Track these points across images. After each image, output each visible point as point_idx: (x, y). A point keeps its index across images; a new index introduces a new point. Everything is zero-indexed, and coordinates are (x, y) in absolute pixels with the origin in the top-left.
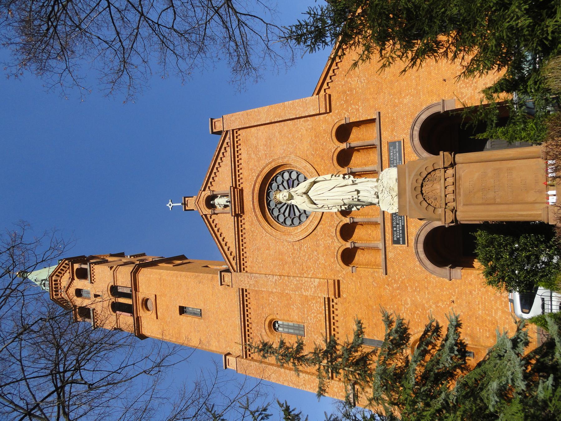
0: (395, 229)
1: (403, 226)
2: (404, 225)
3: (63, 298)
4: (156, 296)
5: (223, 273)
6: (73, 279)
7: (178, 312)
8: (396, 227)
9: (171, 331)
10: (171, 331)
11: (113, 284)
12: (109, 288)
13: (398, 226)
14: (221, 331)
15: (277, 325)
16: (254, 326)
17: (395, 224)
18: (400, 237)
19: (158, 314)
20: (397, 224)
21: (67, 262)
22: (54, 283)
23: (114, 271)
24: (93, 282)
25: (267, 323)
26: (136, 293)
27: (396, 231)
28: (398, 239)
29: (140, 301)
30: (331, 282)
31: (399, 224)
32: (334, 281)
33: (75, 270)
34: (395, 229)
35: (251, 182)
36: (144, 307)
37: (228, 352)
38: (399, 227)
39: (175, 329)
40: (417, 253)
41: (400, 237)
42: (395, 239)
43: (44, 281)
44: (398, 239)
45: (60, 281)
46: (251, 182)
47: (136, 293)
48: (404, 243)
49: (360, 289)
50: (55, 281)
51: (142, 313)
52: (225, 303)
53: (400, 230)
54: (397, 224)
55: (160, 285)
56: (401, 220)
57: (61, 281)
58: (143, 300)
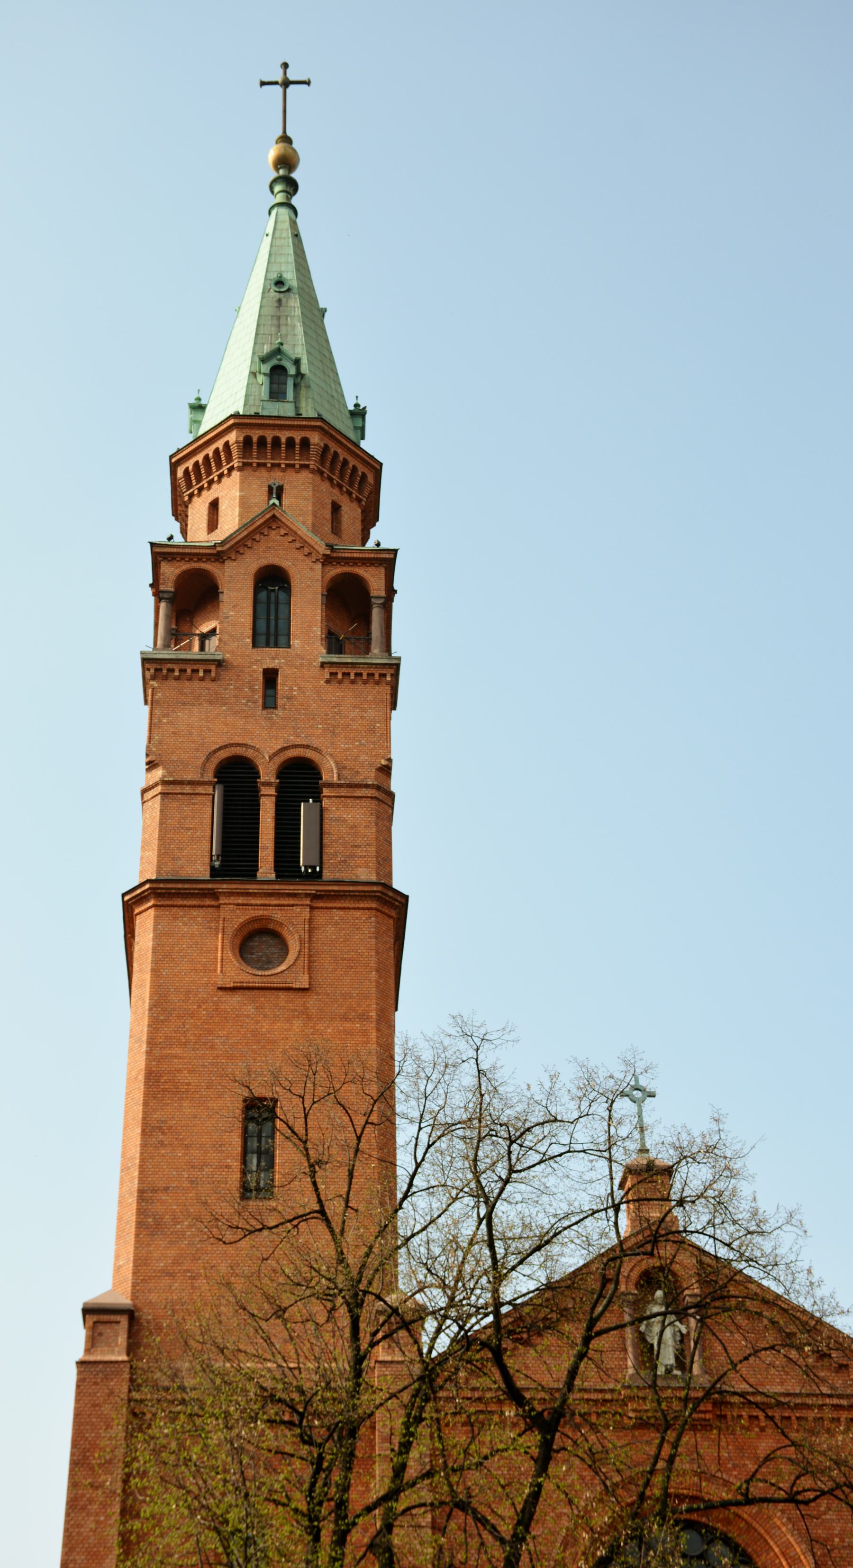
9: (178, 1051)
10: (178, 1051)
26: (307, 895)
29: (278, 915)
33: (361, 571)
35: (735, 1467)
46: (735, 1467)
50: (305, 443)
58: (281, 924)
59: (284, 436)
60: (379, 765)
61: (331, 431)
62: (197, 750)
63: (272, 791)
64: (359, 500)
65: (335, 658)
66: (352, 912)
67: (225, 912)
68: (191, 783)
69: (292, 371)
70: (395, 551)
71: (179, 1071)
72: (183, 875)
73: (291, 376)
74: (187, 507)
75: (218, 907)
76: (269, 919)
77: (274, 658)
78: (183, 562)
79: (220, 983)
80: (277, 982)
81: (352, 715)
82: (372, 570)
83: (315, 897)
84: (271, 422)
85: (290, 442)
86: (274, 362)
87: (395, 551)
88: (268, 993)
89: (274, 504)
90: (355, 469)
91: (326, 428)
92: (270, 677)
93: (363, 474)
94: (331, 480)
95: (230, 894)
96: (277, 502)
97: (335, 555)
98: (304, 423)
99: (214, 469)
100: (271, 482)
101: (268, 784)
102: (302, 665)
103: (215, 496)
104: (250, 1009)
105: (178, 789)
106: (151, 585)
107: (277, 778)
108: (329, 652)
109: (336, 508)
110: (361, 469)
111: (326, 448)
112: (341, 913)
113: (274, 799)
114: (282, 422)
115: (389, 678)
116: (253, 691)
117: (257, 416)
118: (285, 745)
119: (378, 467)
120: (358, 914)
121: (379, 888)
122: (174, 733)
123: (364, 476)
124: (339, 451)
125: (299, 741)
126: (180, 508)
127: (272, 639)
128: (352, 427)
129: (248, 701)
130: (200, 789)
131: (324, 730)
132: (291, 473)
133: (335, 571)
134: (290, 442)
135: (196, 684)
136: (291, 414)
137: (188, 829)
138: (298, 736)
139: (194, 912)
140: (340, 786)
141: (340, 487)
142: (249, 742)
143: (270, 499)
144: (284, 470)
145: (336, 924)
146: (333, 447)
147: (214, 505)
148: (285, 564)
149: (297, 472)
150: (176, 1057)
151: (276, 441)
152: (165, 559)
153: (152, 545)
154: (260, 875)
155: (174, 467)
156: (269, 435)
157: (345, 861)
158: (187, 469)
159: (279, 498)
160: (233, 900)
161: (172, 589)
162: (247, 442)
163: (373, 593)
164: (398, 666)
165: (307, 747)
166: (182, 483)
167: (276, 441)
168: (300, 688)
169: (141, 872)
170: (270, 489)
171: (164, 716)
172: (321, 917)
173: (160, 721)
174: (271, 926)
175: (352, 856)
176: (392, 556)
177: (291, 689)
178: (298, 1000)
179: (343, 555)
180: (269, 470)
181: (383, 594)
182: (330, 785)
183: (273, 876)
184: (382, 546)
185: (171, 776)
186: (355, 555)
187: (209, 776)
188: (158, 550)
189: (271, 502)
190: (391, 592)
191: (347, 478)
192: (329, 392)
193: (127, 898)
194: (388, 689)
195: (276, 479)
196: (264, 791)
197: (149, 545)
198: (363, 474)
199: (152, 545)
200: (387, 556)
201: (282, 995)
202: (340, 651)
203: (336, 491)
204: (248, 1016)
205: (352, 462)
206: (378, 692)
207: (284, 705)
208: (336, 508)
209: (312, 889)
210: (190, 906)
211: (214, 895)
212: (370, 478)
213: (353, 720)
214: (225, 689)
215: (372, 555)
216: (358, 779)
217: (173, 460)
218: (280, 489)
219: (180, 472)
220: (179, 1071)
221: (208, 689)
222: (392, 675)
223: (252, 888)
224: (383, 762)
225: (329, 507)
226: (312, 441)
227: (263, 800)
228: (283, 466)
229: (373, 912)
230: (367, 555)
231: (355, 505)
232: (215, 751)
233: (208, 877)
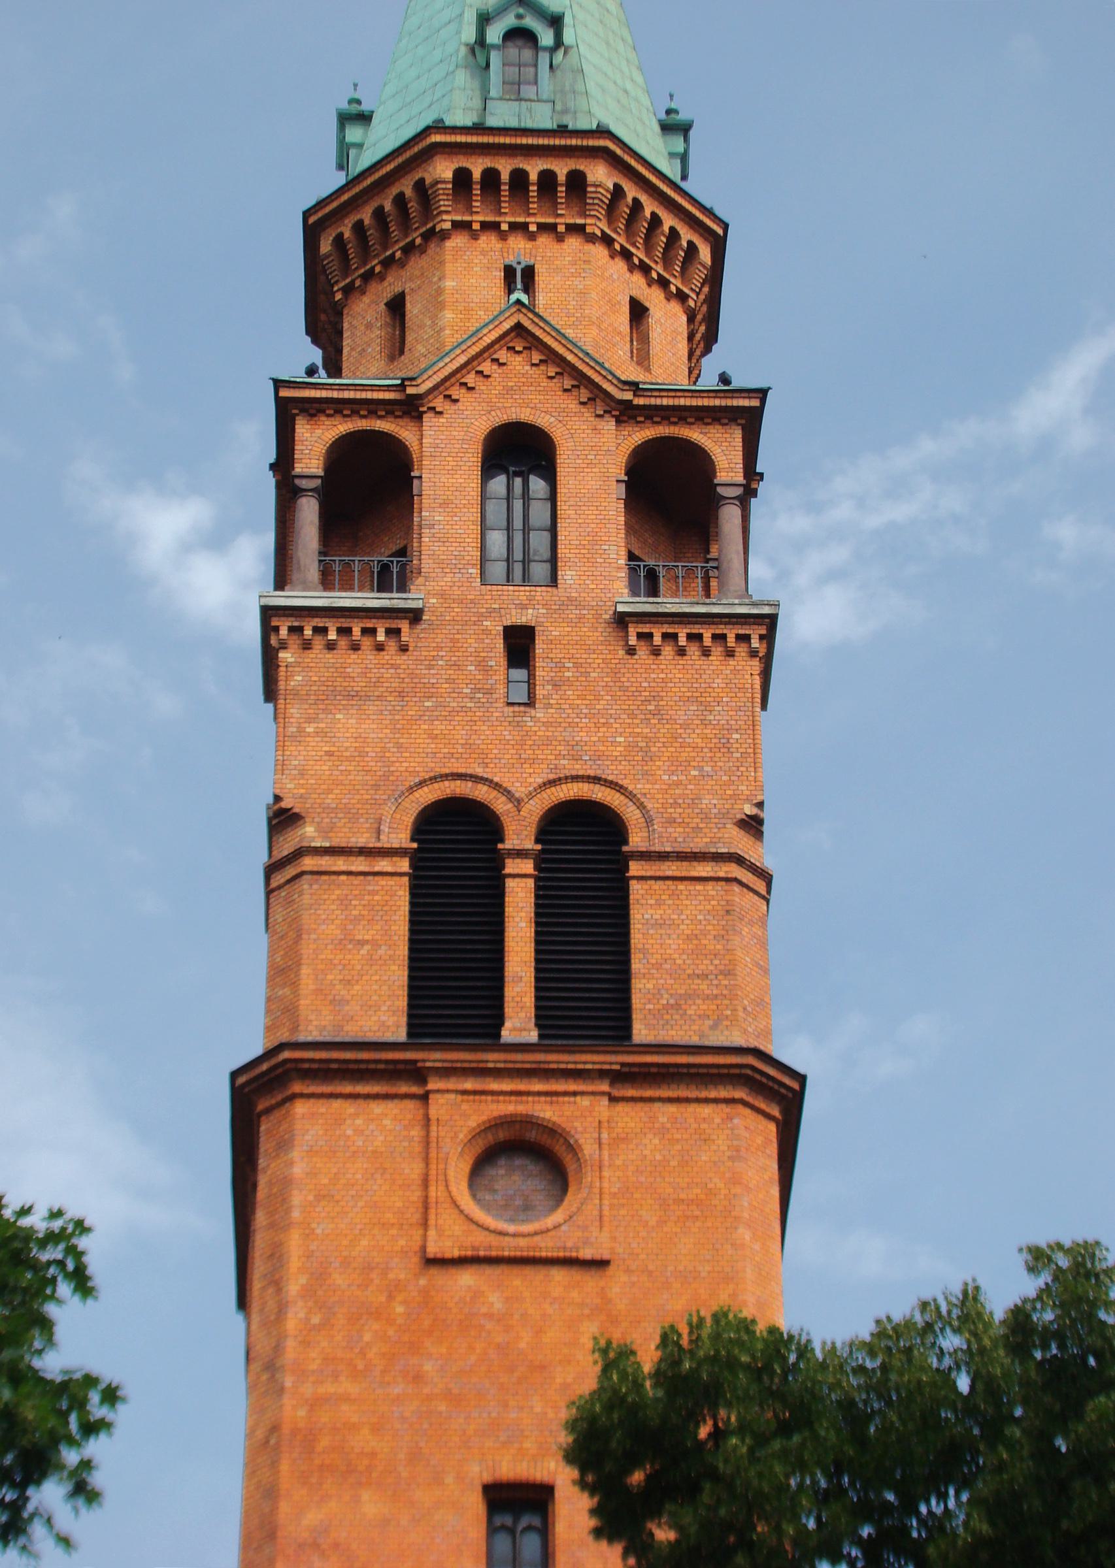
4: (600, 1264)
6: (625, 413)
9: (346, 1386)
10: (346, 1386)
11: (637, 840)
12: (600, 794)
19: (466, 1278)
22: (561, 169)
23: (739, 860)
24: (633, 631)
26: (602, 1074)
29: (546, 1111)
33: (695, 434)
36: (502, 1135)
39: (376, 1429)
45: (577, 229)
47: (602, 1074)
50: (577, 182)
58: (553, 1131)
59: (534, 168)
60: (739, 816)
61: (627, 158)
62: (376, 787)
63: (528, 866)
64: (681, 297)
65: (644, 605)
66: (692, 1108)
68: (364, 852)
69: (546, 38)
70: (762, 393)
71: (354, 1428)
72: (351, 1032)
73: (545, 49)
74: (340, 314)
75: (425, 1098)
76: (528, 1122)
77: (524, 607)
78: (338, 418)
79: (433, 1250)
80: (547, 1247)
81: (681, 717)
82: (716, 431)
83: (620, 1077)
84: (508, 140)
85: (547, 180)
86: (509, 21)
87: (762, 393)
88: (529, 1271)
89: (518, 302)
90: (674, 234)
91: (619, 152)
93: (690, 243)
94: (626, 255)
95: (448, 1072)
96: (524, 298)
97: (641, 401)
98: (574, 142)
99: (395, 234)
100: (511, 260)
101: (520, 854)
102: (581, 618)
103: (398, 289)
104: (495, 1301)
105: (340, 864)
106: (273, 467)
107: (538, 841)
108: (634, 592)
109: (638, 312)
110: (686, 235)
111: (618, 192)
112: (672, 1109)
113: (531, 883)
114: (530, 141)
115: (755, 643)
117: (479, 128)
118: (552, 777)
119: (720, 232)
120: (706, 1110)
121: (750, 1060)
122: (330, 754)
123: (692, 249)
124: (644, 198)
125: (579, 769)
126: (323, 317)
127: (518, 569)
128: (666, 154)
129: (476, 690)
130: (384, 865)
131: (629, 746)
134: (547, 180)
135: (367, 655)
136: (548, 124)
137: (362, 943)
138: (576, 759)
139: (377, 1108)
140: (663, 856)
141: (645, 269)
142: (479, 771)
143: (510, 290)
144: (532, 237)
145: (662, 1132)
146: (631, 192)
147: (397, 307)
148: (543, 421)
149: (560, 239)
150: (346, 1398)
151: (519, 178)
152: (303, 411)
153: (278, 384)
154: (508, 1035)
155: (312, 234)
156: (505, 167)
157: (677, 1006)
158: (339, 238)
159: (529, 286)
160: (452, 1084)
161: (321, 472)
162: (462, 178)
163: (722, 477)
164: (771, 621)
165: (596, 780)
166: (334, 266)
167: (519, 178)
168: (577, 665)
169: (268, 1029)
170: (509, 272)
171: (310, 720)
172: (628, 1117)
173: (301, 730)
174: (532, 1135)
175: (690, 996)
176: (755, 403)
177: (560, 666)
178: (590, 1281)
179: (658, 402)
180: (503, 236)
181: (740, 478)
182: (645, 856)
183: (533, 1036)
184: (736, 383)
185: (326, 838)
186: (682, 402)
187: (400, 836)
188: (284, 393)
189: (514, 297)
190: (752, 474)
191: (659, 251)
192: (619, 82)
193: (241, 1080)
194: (756, 665)
195: (518, 250)
196: (511, 866)
197: (271, 383)
198: (690, 243)
199: (278, 384)
200: (745, 403)
201: (559, 1275)
202: (653, 591)
203: (638, 279)
204: (490, 1316)
205: (669, 221)
206: (735, 671)
207: (548, 697)
208: (638, 312)
209: (613, 1060)
210: (368, 1097)
211: (418, 1074)
212: (705, 253)
213: (685, 726)
214: (430, 667)
215: (717, 402)
216: (698, 844)
217: (311, 220)
218: (529, 273)
219: (326, 246)
220: (354, 1428)
221: (396, 667)
222: (761, 637)
223: (493, 1059)
224: (749, 810)
225: (626, 309)
226: (590, 178)
227: (510, 884)
228: (533, 228)
229: (741, 1109)
230: (706, 402)
231: (675, 308)
232: (411, 790)
233: (401, 1035)
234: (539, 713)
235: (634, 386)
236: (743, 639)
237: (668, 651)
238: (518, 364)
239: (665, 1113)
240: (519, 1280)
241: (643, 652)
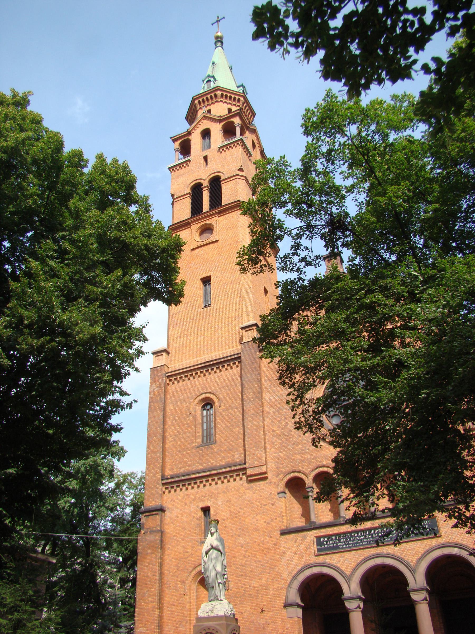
0: (334, 538)
1: (337, 547)
2: (339, 548)
3: (197, 112)
4: (217, 241)
5: (255, 328)
6: (220, 121)
7: (204, 275)
8: (336, 539)
11: (222, 178)
13: (338, 541)
14: (191, 338)
15: (208, 407)
16: (202, 379)
17: (340, 537)
18: (324, 545)
19: (198, 250)
20: (340, 540)
21: (242, 99)
23: (238, 175)
25: (208, 395)
26: (216, 213)
27: (332, 540)
28: (322, 544)
30: (264, 469)
31: (340, 542)
32: (265, 473)
34: (334, 538)
37: (170, 352)
38: (337, 543)
40: (310, 566)
41: (324, 545)
42: (322, 540)
43: (212, 79)
44: (322, 544)
47: (216, 213)
48: (319, 550)
49: (261, 504)
50: (215, 95)
51: (195, 227)
52: (223, 337)
53: (333, 544)
54: (340, 540)
55: (230, 245)
56: (345, 544)
57: (216, 104)
58: (210, 224)
67: (193, 227)
69: (212, 79)
86: (207, 80)
92: (206, 158)
101: (205, 187)
116: (200, 163)
120: (233, 213)
132: (212, 105)
133: (223, 123)
146: (225, 94)
178: (216, 244)
182: (224, 180)
195: (209, 108)
234: (208, 166)
235: (220, 116)
236: (238, 144)
237: (227, 150)
238: (205, 121)
239: (226, 216)
240: (205, 248)
241: (223, 152)
